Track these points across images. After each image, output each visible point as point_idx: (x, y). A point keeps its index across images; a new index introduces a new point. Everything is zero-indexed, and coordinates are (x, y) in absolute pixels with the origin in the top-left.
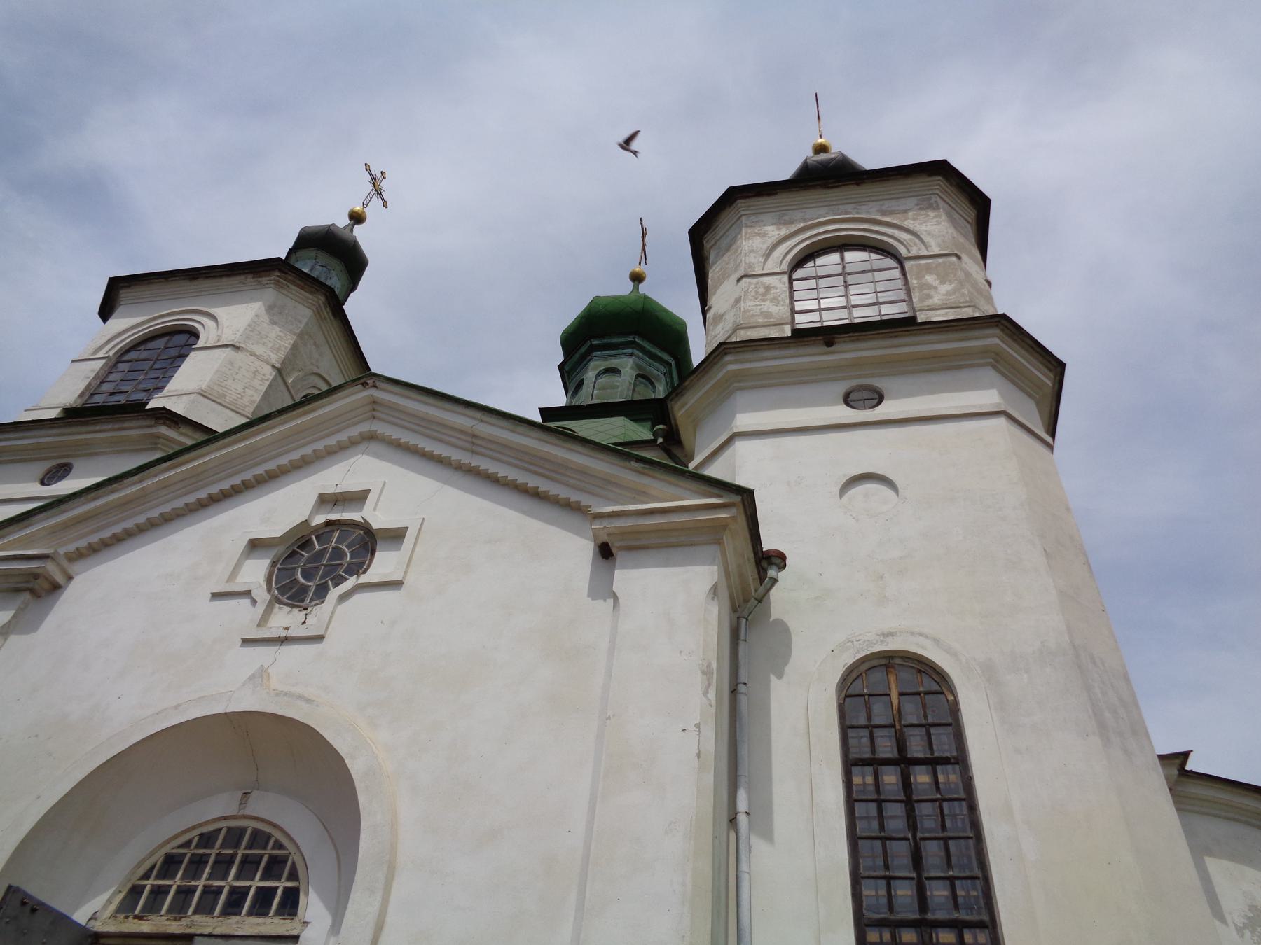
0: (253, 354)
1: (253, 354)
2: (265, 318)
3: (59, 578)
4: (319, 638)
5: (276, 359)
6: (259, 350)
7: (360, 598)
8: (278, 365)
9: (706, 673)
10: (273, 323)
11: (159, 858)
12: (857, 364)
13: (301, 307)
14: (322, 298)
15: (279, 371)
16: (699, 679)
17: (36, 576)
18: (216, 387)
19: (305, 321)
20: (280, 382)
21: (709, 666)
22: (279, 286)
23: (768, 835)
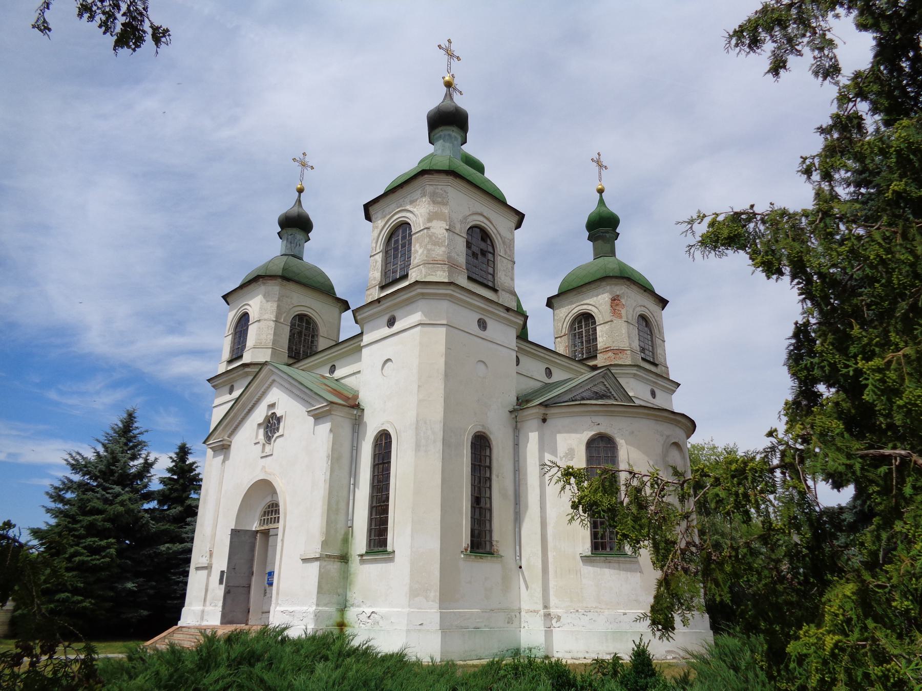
0: (265, 320)
1: (265, 320)
2: (264, 301)
3: (229, 443)
4: (272, 455)
5: (273, 318)
6: (266, 317)
7: (278, 440)
8: (274, 319)
9: (328, 457)
10: (268, 301)
11: (263, 513)
12: (388, 308)
13: (274, 287)
14: (280, 280)
15: (276, 321)
16: (326, 458)
17: (223, 445)
18: (258, 341)
19: (278, 293)
20: (279, 324)
21: (329, 454)
22: (264, 284)
23: (358, 488)
